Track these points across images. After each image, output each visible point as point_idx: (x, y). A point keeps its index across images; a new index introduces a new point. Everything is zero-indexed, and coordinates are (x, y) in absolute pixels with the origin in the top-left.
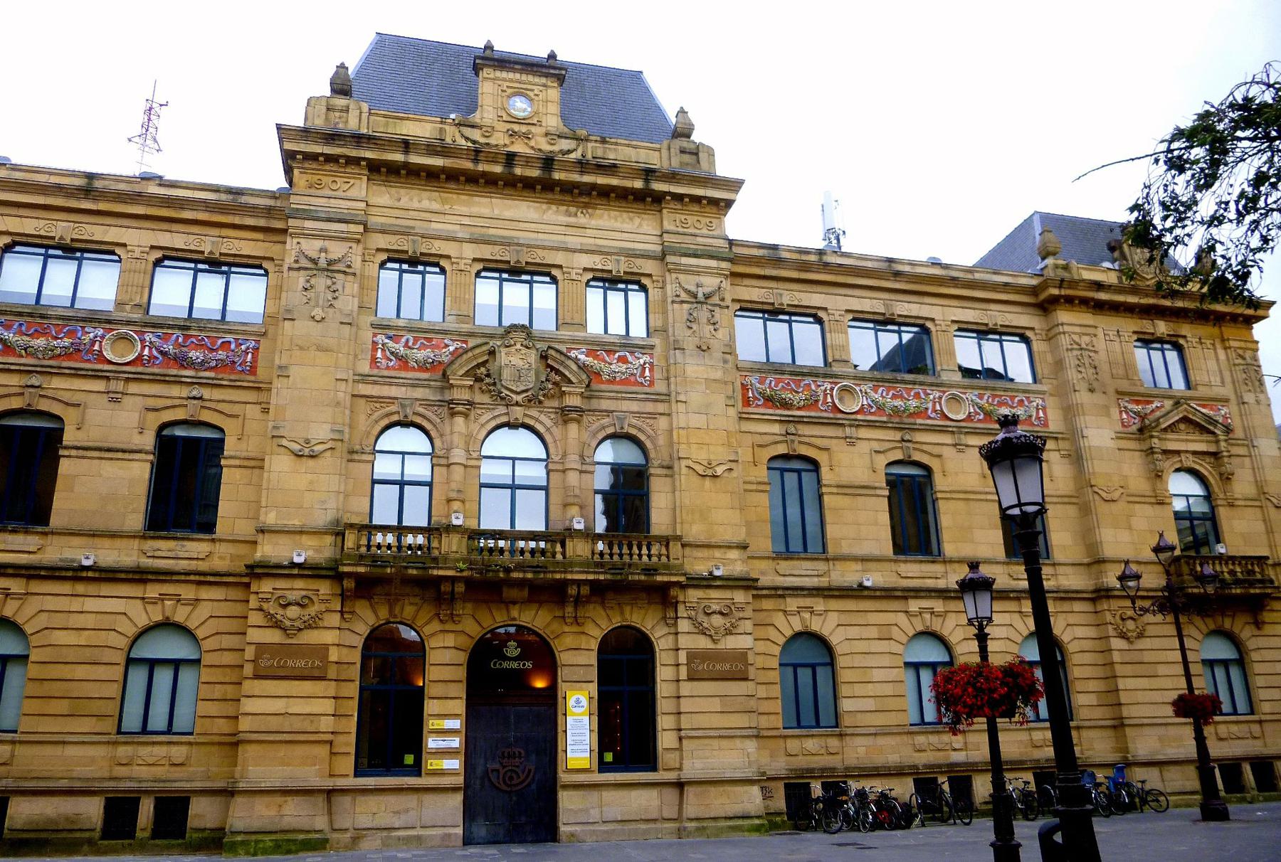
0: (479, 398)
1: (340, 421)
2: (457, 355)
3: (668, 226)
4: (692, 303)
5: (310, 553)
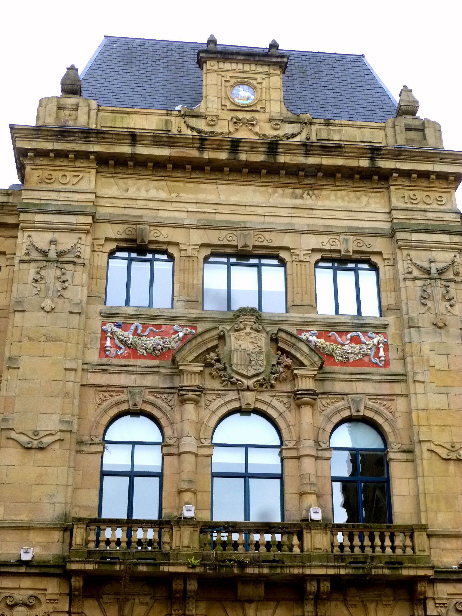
0: (210, 384)
1: (69, 411)
2: (186, 340)
3: (396, 202)
4: (425, 279)
5: (38, 550)
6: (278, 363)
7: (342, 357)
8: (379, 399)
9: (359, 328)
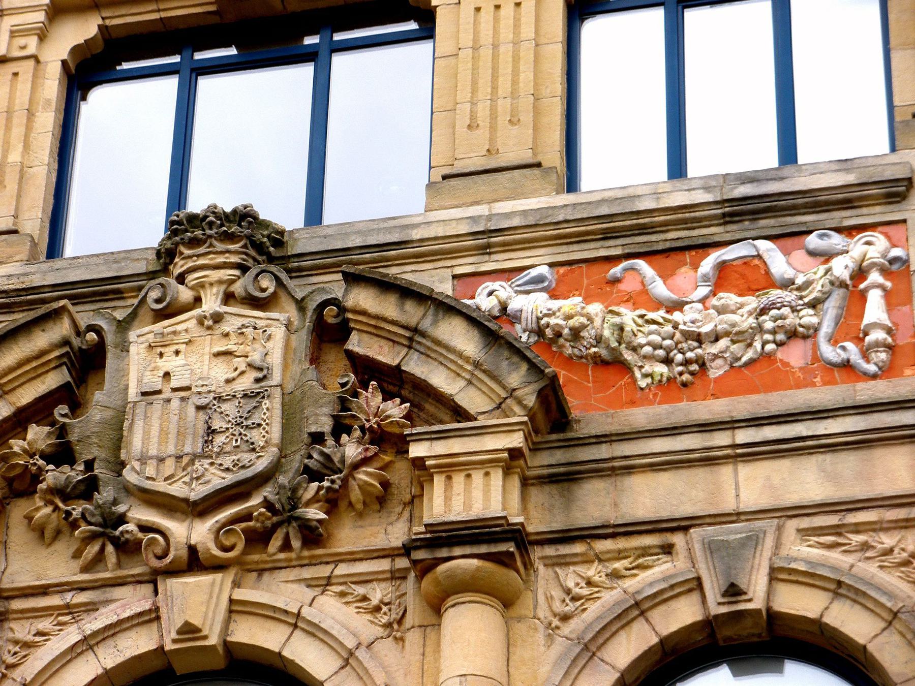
6: (340, 428)
7: (668, 361)
8: (857, 528)
9: (763, 223)
